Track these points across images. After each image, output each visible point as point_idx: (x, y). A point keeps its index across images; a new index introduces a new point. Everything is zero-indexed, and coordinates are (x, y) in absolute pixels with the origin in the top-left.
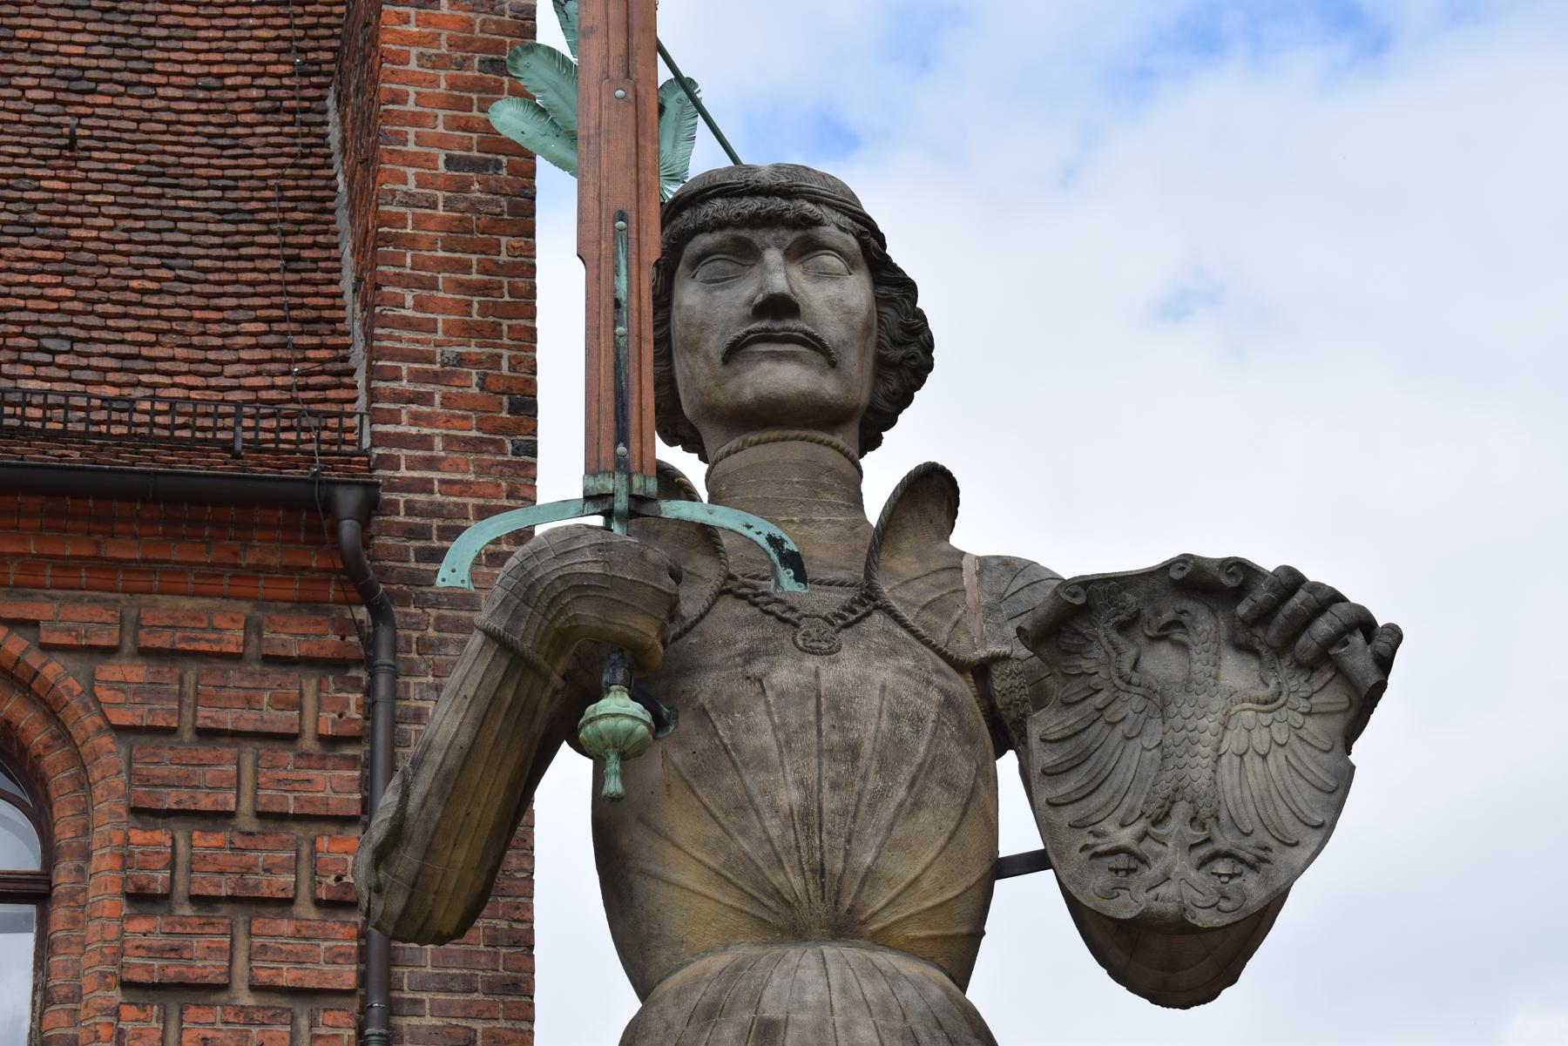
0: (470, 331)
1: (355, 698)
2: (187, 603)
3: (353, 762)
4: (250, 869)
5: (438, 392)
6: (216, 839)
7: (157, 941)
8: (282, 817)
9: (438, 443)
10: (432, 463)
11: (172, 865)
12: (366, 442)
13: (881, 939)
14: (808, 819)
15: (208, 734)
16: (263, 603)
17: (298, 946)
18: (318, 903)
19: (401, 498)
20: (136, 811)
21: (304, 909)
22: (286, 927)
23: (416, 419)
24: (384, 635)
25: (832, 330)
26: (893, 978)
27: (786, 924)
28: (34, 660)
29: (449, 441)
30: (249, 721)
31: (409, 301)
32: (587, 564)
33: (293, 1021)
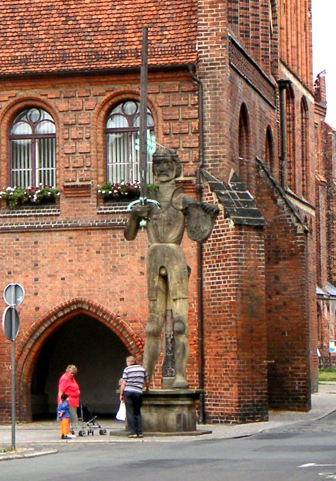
0: (215, 24)
1: (196, 97)
2: (170, 83)
3: (196, 108)
4: (181, 128)
5: (208, 37)
6: (177, 124)
7: (168, 141)
8: (186, 119)
9: (209, 47)
10: (208, 51)
11: (170, 129)
12: (197, 49)
15: (173, 106)
16: (181, 81)
17: (189, 140)
18: (193, 133)
19: (203, 59)
20: (164, 120)
21: (190, 134)
22: (187, 137)
23: (205, 43)
24: (200, 86)
29: (211, 47)
31: (203, 20)
33: (189, 153)
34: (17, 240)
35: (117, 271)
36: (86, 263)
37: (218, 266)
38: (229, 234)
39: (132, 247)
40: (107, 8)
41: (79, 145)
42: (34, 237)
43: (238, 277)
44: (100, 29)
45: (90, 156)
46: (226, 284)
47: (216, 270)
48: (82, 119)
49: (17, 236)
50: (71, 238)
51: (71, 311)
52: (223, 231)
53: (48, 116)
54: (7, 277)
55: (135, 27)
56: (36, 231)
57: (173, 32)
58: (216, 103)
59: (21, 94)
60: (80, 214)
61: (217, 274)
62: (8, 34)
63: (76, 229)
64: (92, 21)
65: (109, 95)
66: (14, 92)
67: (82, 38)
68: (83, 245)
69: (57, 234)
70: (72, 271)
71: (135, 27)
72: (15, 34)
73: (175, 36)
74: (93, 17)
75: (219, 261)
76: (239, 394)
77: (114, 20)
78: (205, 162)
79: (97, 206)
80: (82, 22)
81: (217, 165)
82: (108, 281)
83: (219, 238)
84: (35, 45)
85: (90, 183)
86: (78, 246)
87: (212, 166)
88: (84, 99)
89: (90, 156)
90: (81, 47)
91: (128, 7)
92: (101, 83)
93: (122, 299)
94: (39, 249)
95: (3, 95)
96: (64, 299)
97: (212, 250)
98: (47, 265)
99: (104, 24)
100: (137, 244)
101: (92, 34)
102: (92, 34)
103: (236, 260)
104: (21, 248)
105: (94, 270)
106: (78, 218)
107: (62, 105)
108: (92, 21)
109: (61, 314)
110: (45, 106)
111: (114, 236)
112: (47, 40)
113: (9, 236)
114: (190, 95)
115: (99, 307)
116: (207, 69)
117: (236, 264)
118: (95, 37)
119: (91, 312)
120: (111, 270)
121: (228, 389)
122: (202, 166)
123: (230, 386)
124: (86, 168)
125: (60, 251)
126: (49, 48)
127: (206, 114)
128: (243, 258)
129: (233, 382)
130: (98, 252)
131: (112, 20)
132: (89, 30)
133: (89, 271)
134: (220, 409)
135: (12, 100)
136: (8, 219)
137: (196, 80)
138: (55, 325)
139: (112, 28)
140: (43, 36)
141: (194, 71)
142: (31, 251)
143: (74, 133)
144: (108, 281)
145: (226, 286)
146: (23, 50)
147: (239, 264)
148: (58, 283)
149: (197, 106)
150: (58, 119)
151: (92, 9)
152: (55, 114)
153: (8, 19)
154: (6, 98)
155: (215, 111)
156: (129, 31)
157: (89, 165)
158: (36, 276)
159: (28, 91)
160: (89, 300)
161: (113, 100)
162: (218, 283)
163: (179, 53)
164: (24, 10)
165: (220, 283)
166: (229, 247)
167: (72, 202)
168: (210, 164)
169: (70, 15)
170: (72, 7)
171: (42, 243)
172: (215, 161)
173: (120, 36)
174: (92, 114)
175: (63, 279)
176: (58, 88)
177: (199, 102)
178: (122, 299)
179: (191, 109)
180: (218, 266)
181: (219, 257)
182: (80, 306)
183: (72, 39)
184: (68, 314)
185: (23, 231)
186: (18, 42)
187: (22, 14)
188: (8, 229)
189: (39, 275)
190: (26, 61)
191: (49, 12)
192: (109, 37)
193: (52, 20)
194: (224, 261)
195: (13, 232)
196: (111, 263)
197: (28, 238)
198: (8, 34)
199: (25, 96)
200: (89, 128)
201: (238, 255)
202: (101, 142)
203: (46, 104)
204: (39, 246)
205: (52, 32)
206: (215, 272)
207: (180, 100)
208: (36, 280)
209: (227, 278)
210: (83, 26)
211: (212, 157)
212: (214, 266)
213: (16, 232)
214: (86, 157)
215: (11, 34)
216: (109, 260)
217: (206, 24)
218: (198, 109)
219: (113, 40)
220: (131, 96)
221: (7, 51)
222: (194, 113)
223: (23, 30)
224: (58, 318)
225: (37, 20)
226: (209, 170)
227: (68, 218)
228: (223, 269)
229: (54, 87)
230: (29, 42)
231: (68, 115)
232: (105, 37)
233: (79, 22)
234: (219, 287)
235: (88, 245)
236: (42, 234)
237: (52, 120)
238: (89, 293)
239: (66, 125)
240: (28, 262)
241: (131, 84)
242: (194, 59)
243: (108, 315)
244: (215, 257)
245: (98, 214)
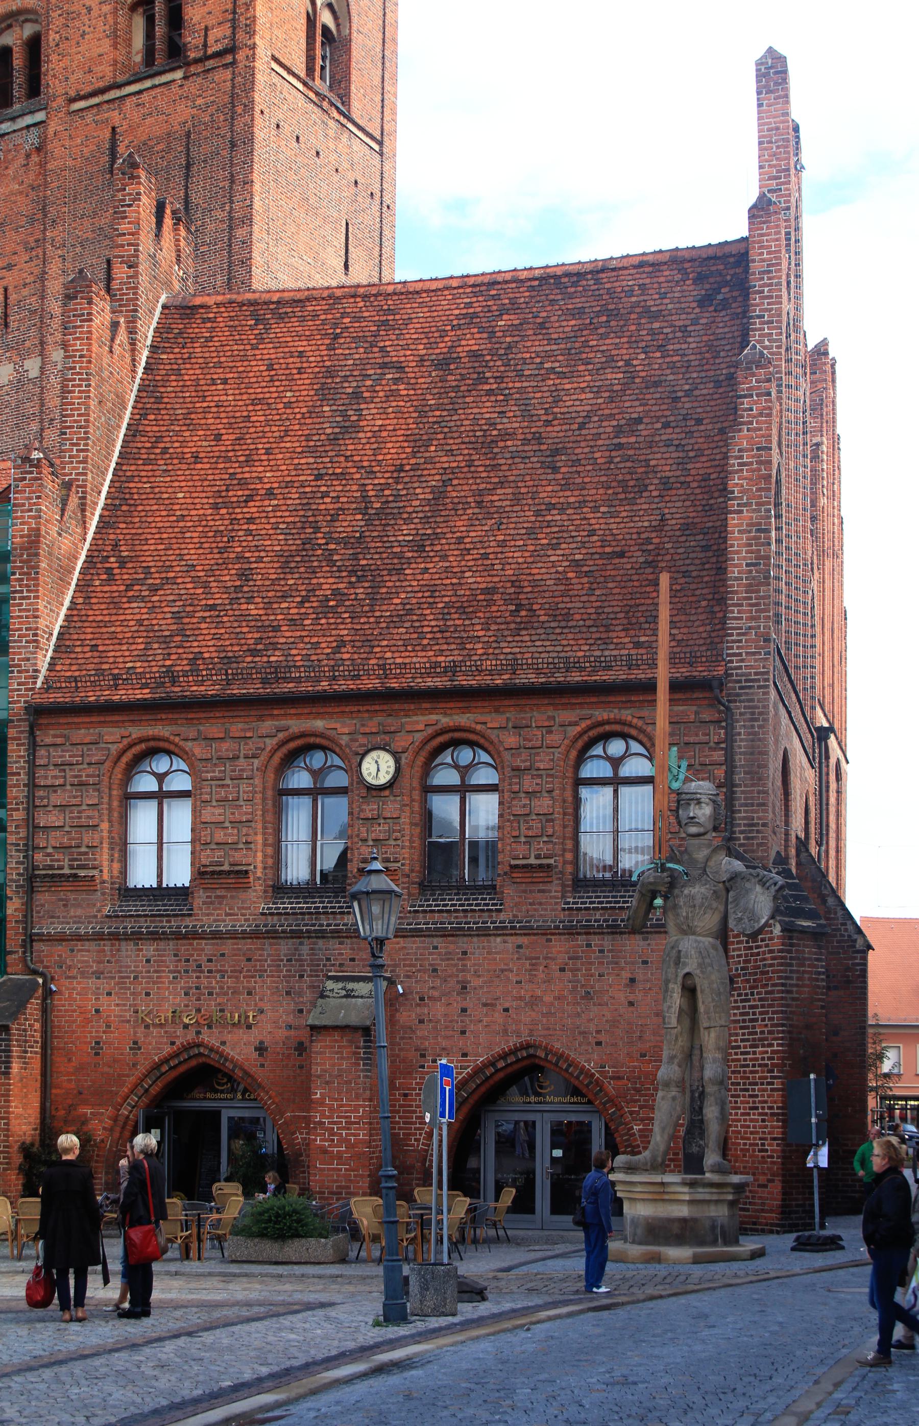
0: (752, 618)
2: (681, 708)
3: (722, 749)
13: (699, 935)
14: (687, 918)
16: (699, 706)
25: (702, 820)
26: (699, 942)
27: (684, 933)
28: (645, 727)
30: (697, 739)
32: (651, 880)
34: (435, 948)
35: (592, 998)
36: (544, 986)
37: (752, 994)
38: (773, 945)
39: (617, 963)
40: (581, 593)
41: (535, 802)
42: (463, 943)
43: (785, 1012)
44: (570, 624)
45: (552, 820)
47: (749, 1000)
48: (541, 761)
49: (436, 941)
50: (520, 947)
51: (518, 1061)
53: (484, 757)
54: (418, 1005)
55: (625, 622)
56: (465, 935)
57: (685, 630)
58: (753, 741)
59: (445, 721)
60: (535, 910)
61: (751, 1007)
62: (426, 630)
63: (528, 931)
64: (558, 612)
65: (584, 725)
66: (434, 717)
67: (543, 637)
68: (538, 958)
69: (499, 939)
70: (521, 998)
71: (625, 622)
72: (435, 629)
73: (690, 636)
74: (560, 606)
75: (757, 987)
76: (784, 1194)
77: (593, 611)
78: (734, 833)
79: (563, 897)
80: (542, 612)
81: (752, 838)
82: (578, 1015)
84: (468, 646)
85: (551, 861)
86: (531, 958)
87: (745, 838)
88: (544, 730)
89: (552, 820)
90: (540, 649)
91: (615, 591)
92: (573, 706)
93: (599, 1044)
94: (469, 963)
95: (417, 722)
96: (508, 1042)
97: (742, 969)
98: (482, 987)
99: (577, 617)
100: (625, 957)
101: (558, 631)
102: (558, 631)
103: (783, 985)
104: (442, 960)
105: (555, 998)
106: (532, 916)
107: (511, 740)
108: (558, 612)
109: (501, 1064)
110: (482, 741)
111: (588, 945)
112: (486, 639)
113: (423, 942)
114: (712, 728)
115: (562, 1055)
116: (741, 688)
117: (782, 992)
118: (563, 636)
119: (550, 1062)
120: (582, 998)
121: (765, 1186)
122: (730, 839)
123: (769, 1181)
124: (545, 839)
125: (503, 967)
126: (491, 651)
127: (737, 757)
128: (794, 982)
129: (773, 1175)
130: (562, 970)
131: (589, 611)
132: (553, 625)
133: (548, 999)
134: (750, 1216)
135: (430, 730)
136: (421, 915)
137: (723, 705)
138: (491, 1082)
139: (588, 623)
140: (481, 633)
141: (721, 691)
142: (456, 965)
143: (528, 783)
144: (578, 1015)
145: (766, 1026)
146: (448, 653)
147: (788, 992)
148: (498, 1017)
149: (723, 745)
150: (502, 761)
151: (556, 594)
152: (499, 753)
153: (426, 606)
154: (421, 727)
155: (752, 753)
156: (617, 628)
157: (550, 833)
158: (464, 1004)
159: (456, 717)
160: (547, 1044)
161: (591, 734)
162: (751, 1020)
163: (696, 662)
164: (449, 593)
165: (756, 1020)
166: (771, 965)
167: (525, 891)
168: (742, 836)
169: (523, 602)
170: (525, 590)
171: (474, 954)
172: (751, 831)
173: (603, 636)
174: (557, 754)
175: (506, 1010)
176: (504, 712)
177: (726, 739)
178: (599, 1044)
179: (714, 749)
180: (752, 994)
181: (755, 980)
182: (531, 1051)
183: (527, 638)
184: (511, 1064)
185: (444, 934)
186: (440, 641)
187: (447, 599)
188: (421, 930)
189: (469, 1003)
190: (452, 669)
191: (489, 597)
192: (584, 636)
193: (494, 608)
195: (429, 936)
196: (582, 986)
197: (452, 946)
198: (426, 630)
199: (451, 724)
200: (552, 776)
201: (786, 978)
202: (570, 799)
203: (483, 736)
204: (469, 959)
205: (493, 627)
207: (697, 735)
208: (464, 1010)
209: (767, 1012)
210: (542, 619)
211: (745, 825)
212: (746, 995)
213: (432, 936)
214: (547, 821)
215: (429, 629)
216: (578, 981)
217: (741, 618)
218: (725, 749)
219: (592, 641)
220: (618, 728)
221: (424, 654)
222: (719, 756)
223: (448, 623)
224: (497, 1071)
225: (471, 609)
226: (741, 845)
227: (515, 916)
228: (760, 1000)
229: (497, 711)
230: (459, 641)
231: (519, 755)
232: (579, 636)
233: (538, 613)
234: (754, 1027)
235: (546, 958)
236: (475, 939)
237: (492, 762)
238: (546, 1032)
239: (516, 769)
240: (452, 982)
241: (620, 709)
242: (721, 671)
243: (576, 1067)
244: (748, 981)
245: (564, 909)
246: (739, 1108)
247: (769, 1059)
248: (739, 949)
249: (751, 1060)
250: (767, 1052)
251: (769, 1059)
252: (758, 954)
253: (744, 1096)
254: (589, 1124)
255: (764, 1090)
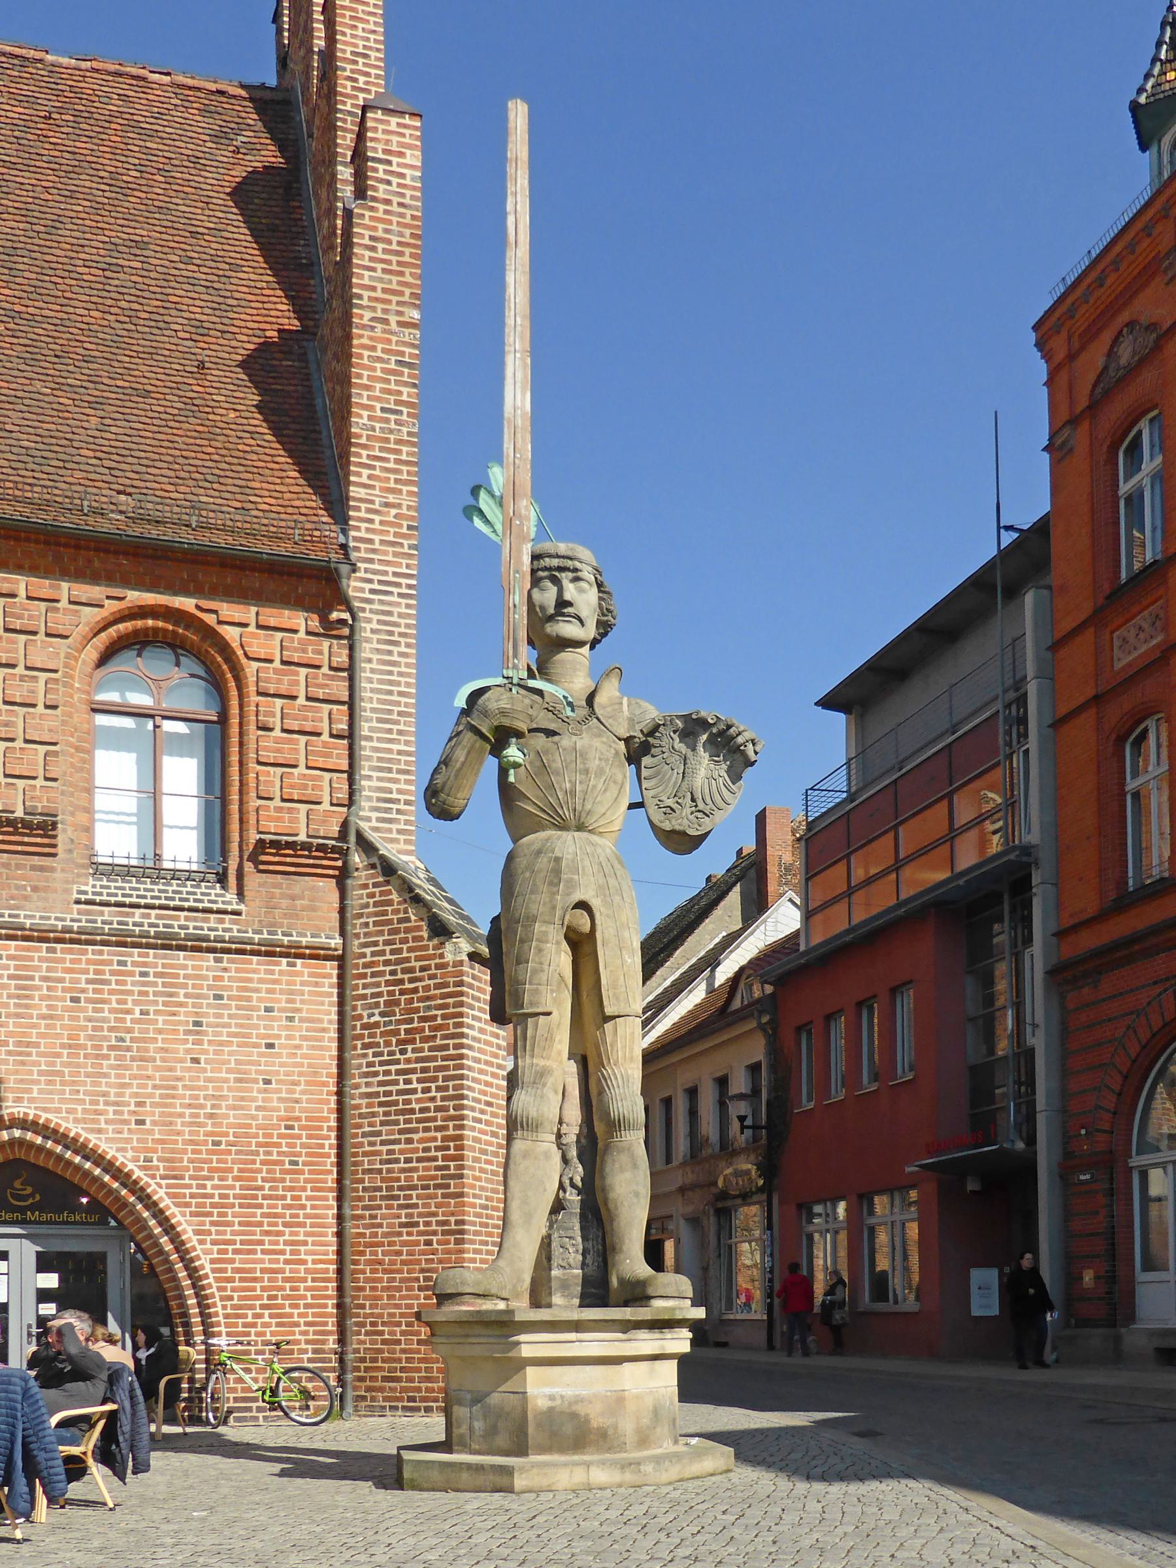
10: (374, 551)
23: (368, 530)
46: (433, 1094)
47: (398, 1062)
52: (423, 969)
83: (407, 986)
145: (433, 1099)
165: (414, 1091)
194: (425, 1040)
206: (393, 1068)
212: (391, 1053)
246: (380, 1226)
247: (437, 1149)
248: (378, 985)
249: (401, 1152)
250: (435, 1139)
251: (437, 1149)
252: (415, 990)
253: (389, 1207)
254: (102, 1257)
255: (430, 1197)
